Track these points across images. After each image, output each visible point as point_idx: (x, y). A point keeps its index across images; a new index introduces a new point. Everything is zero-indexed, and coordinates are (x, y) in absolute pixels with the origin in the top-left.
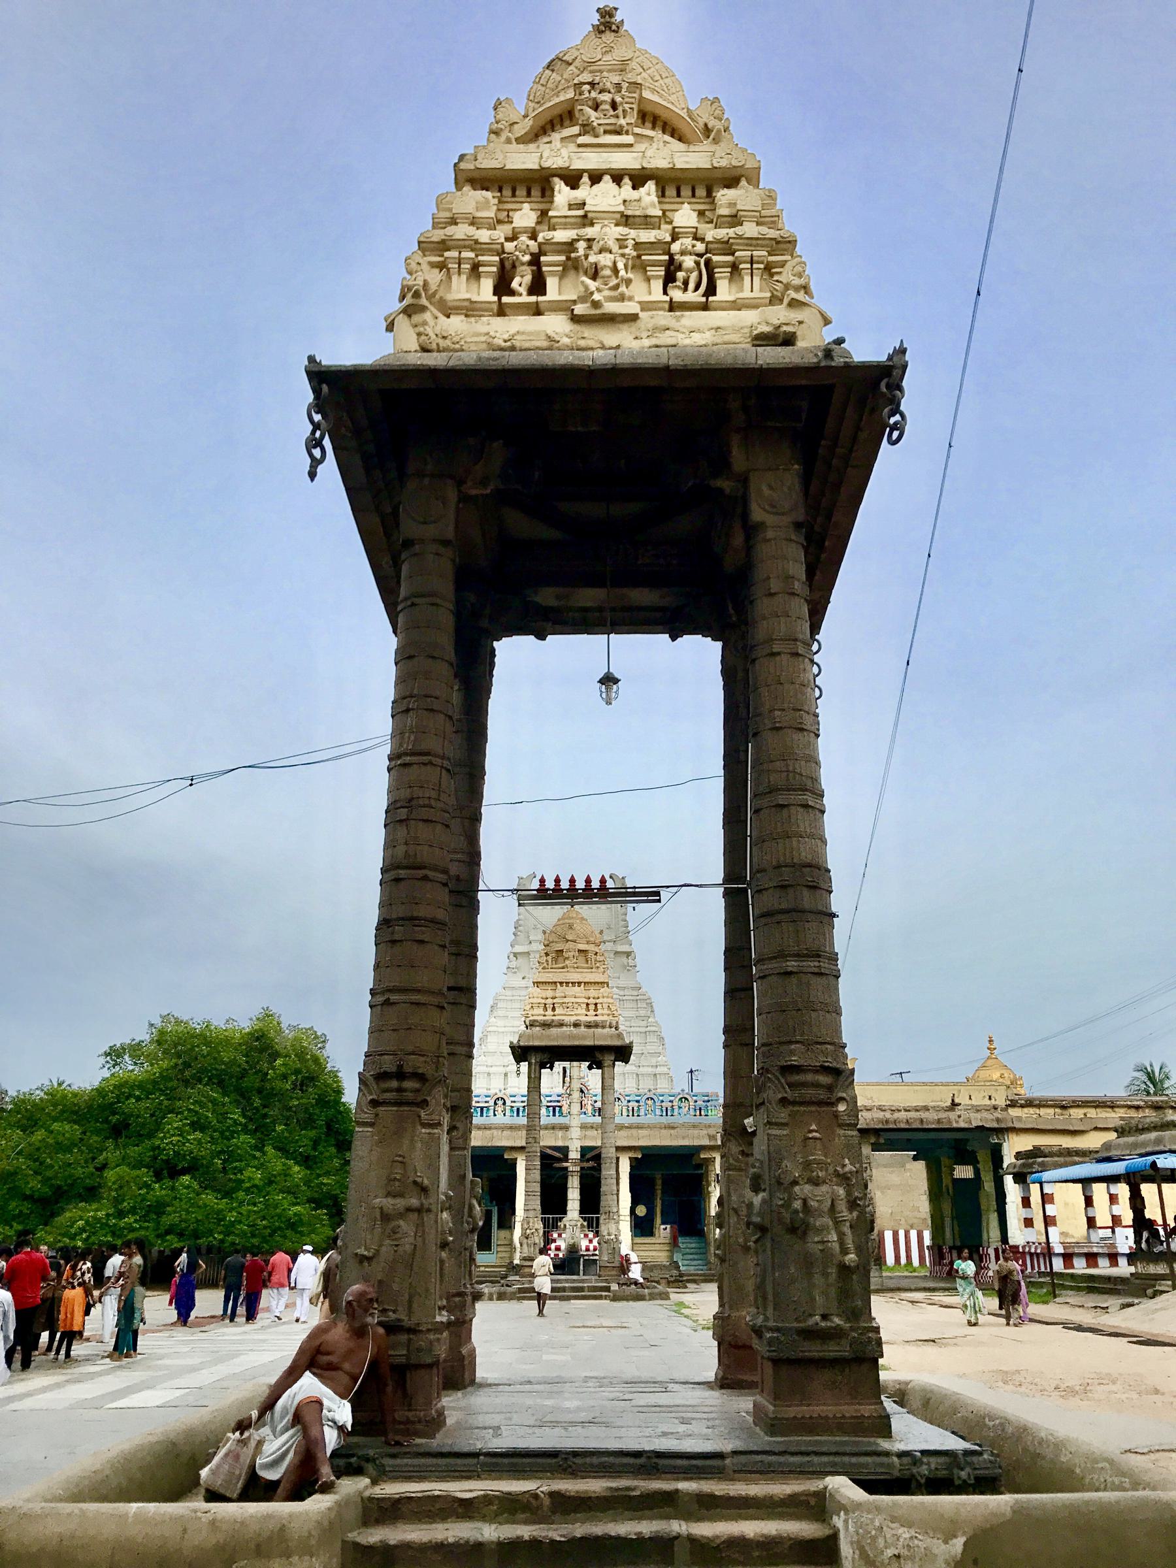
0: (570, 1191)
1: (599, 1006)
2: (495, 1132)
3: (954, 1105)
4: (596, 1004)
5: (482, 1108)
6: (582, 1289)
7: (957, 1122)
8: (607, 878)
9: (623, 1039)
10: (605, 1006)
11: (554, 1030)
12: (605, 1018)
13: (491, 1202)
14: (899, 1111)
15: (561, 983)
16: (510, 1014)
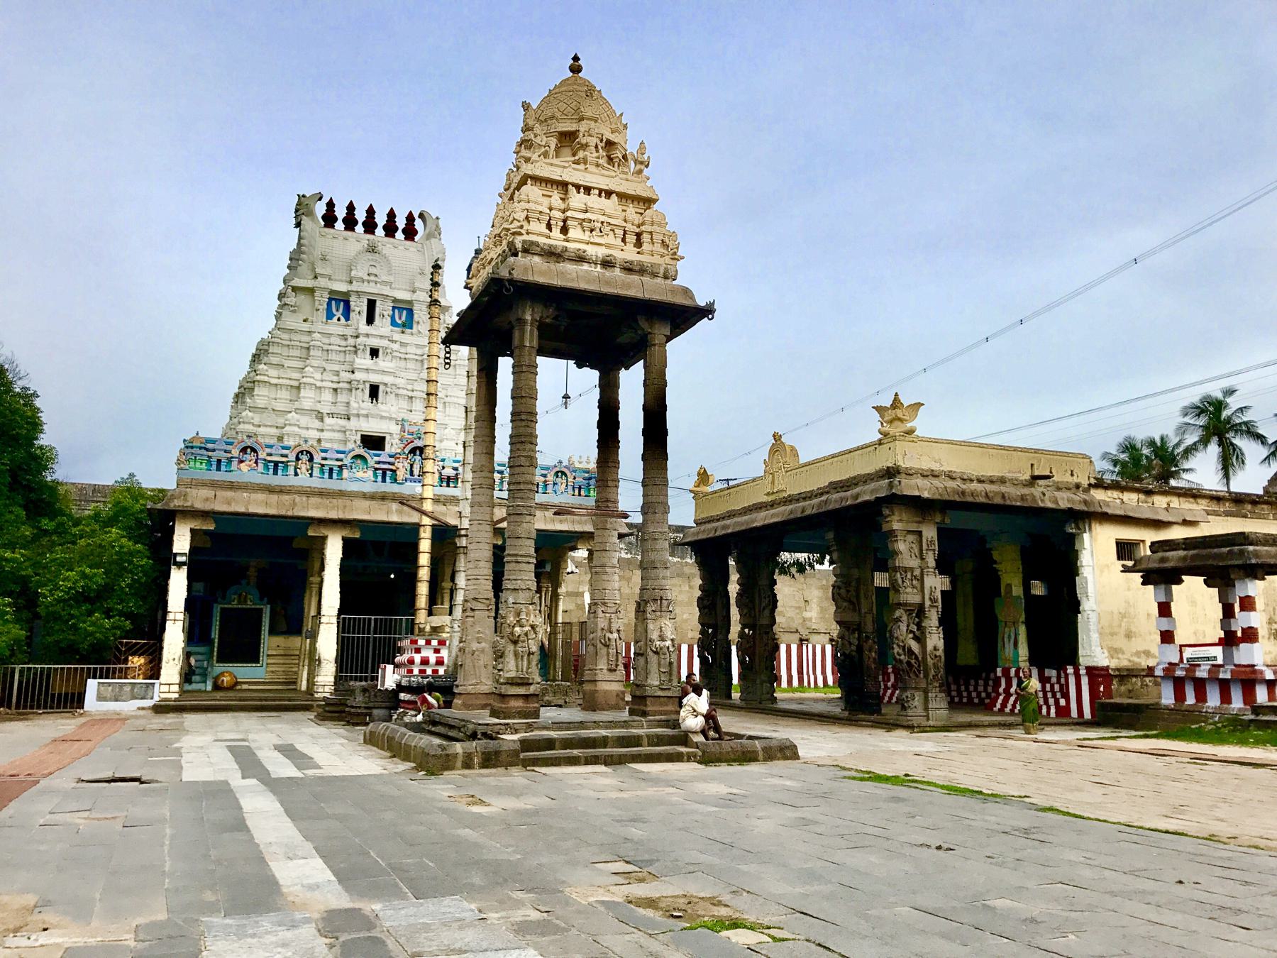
2: (297, 498)
3: (1035, 478)
4: (639, 235)
5: (276, 464)
8: (416, 216)
9: (692, 298)
11: (569, 267)
12: (656, 259)
13: (261, 599)
14: (972, 481)
15: (578, 187)
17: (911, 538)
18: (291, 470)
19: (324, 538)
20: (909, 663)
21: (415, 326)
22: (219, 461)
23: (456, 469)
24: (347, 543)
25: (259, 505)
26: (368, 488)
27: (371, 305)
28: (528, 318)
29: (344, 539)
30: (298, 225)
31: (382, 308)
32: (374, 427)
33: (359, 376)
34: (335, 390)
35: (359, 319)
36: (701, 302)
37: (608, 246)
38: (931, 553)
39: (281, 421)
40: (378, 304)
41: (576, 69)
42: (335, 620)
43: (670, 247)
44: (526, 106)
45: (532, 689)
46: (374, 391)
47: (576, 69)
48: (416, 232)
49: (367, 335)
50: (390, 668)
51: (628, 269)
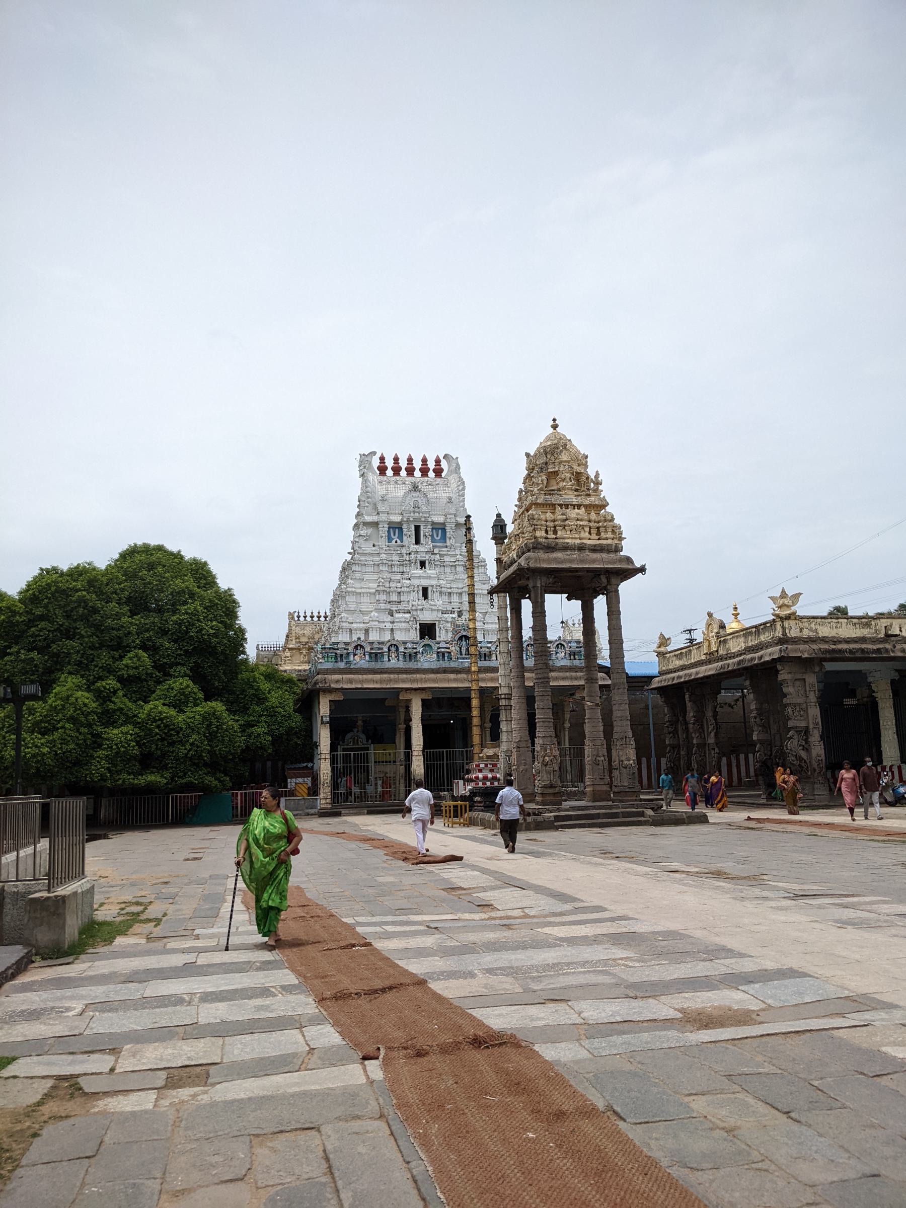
0: (474, 728)
1: (602, 529)
2: (392, 676)
3: (888, 636)
5: (376, 654)
6: (615, 815)
7: (893, 652)
8: (441, 458)
9: (632, 562)
10: (610, 529)
11: (559, 555)
12: (609, 542)
13: (367, 741)
15: (561, 505)
16: (366, 577)
17: (798, 683)
18: (386, 658)
19: (410, 700)
20: (800, 766)
21: (448, 540)
22: (342, 656)
23: (489, 648)
24: (425, 703)
25: (371, 682)
26: (434, 666)
27: (417, 528)
28: (539, 585)
29: (422, 700)
30: (362, 475)
31: (425, 530)
32: (427, 617)
33: (415, 582)
34: (399, 593)
35: (409, 540)
36: (638, 564)
37: (580, 538)
38: (812, 693)
39: (367, 618)
40: (422, 528)
41: (555, 427)
42: (421, 753)
43: (617, 532)
44: (528, 455)
45: (557, 790)
46: (425, 591)
47: (555, 427)
48: (442, 470)
49: (417, 552)
50: (461, 782)
51: (594, 549)
